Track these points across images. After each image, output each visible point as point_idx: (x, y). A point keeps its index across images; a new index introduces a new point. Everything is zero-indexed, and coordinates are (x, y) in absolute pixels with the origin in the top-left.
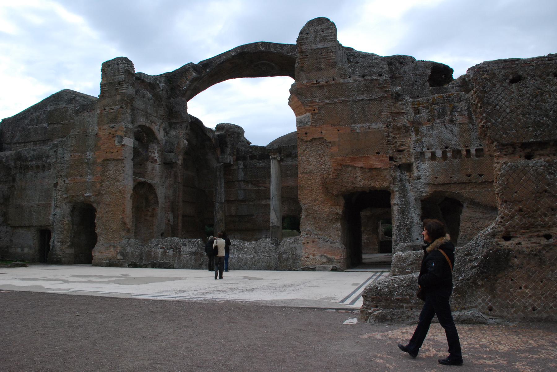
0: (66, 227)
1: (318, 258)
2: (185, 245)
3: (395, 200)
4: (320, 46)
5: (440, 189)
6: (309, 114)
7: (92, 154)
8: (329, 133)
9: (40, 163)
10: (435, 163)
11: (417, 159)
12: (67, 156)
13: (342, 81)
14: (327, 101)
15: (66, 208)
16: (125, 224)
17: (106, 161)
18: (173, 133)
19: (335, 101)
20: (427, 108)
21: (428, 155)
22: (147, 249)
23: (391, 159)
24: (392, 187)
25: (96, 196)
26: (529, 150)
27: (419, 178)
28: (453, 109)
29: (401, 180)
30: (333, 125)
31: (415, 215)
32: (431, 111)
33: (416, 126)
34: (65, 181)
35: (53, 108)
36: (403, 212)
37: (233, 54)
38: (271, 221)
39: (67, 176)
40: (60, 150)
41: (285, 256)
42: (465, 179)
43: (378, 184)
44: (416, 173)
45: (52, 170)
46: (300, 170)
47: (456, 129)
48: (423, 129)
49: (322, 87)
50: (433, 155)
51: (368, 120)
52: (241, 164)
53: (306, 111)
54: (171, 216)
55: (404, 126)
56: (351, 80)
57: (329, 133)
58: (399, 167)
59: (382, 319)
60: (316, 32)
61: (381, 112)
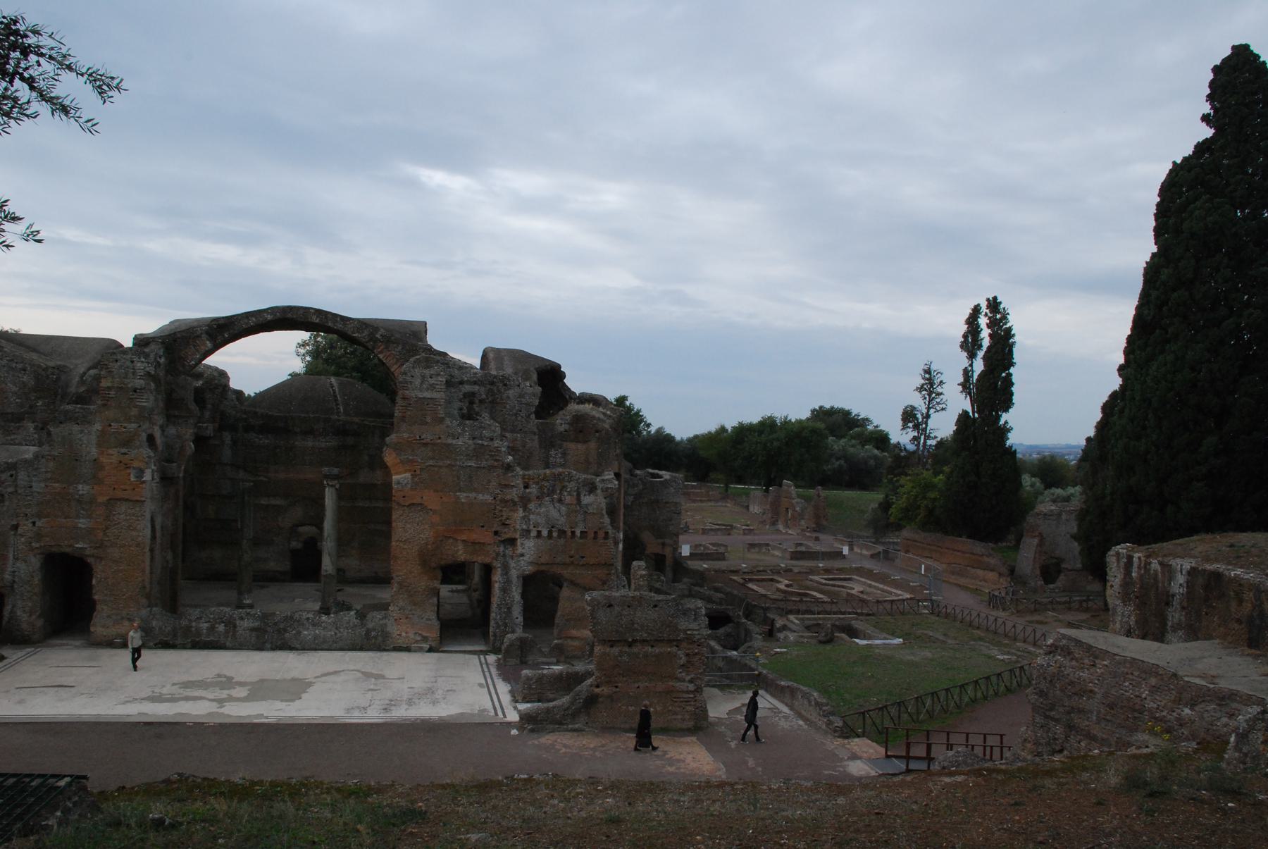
0: (36, 590)
1: (411, 636)
2: (242, 619)
4: (427, 395)
5: (543, 568)
6: (408, 475)
7: (87, 488)
8: (431, 499)
10: (540, 541)
11: (522, 536)
12: (38, 487)
13: (450, 441)
14: (431, 462)
15: (35, 562)
16: (144, 587)
17: (113, 501)
18: (172, 430)
19: (440, 463)
20: (537, 483)
21: (534, 534)
22: (184, 623)
23: (496, 533)
24: (495, 564)
25: (96, 548)
26: (612, 643)
27: (522, 555)
28: (564, 487)
29: (504, 556)
30: (436, 491)
31: (516, 594)
32: (541, 488)
33: (525, 501)
34: (34, 523)
36: (505, 590)
37: (269, 317)
38: (324, 567)
39: (39, 516)
40: (22, 475)
41: (373, 634)
42: (568, 560)
44: (520, 550)
45: (7, 503)
46: (394, 538)
47: (563, 509)
48: (531, 506)
49: (426, 445)
50: (539, 532)
51: (475, 490)
52: (227, 437)
53: (406, 472)
54: (169, 556)
55: (512, 500)
58: (503, 542)
59: (532, 731)
60: (423, 377)
61: (489, 481)
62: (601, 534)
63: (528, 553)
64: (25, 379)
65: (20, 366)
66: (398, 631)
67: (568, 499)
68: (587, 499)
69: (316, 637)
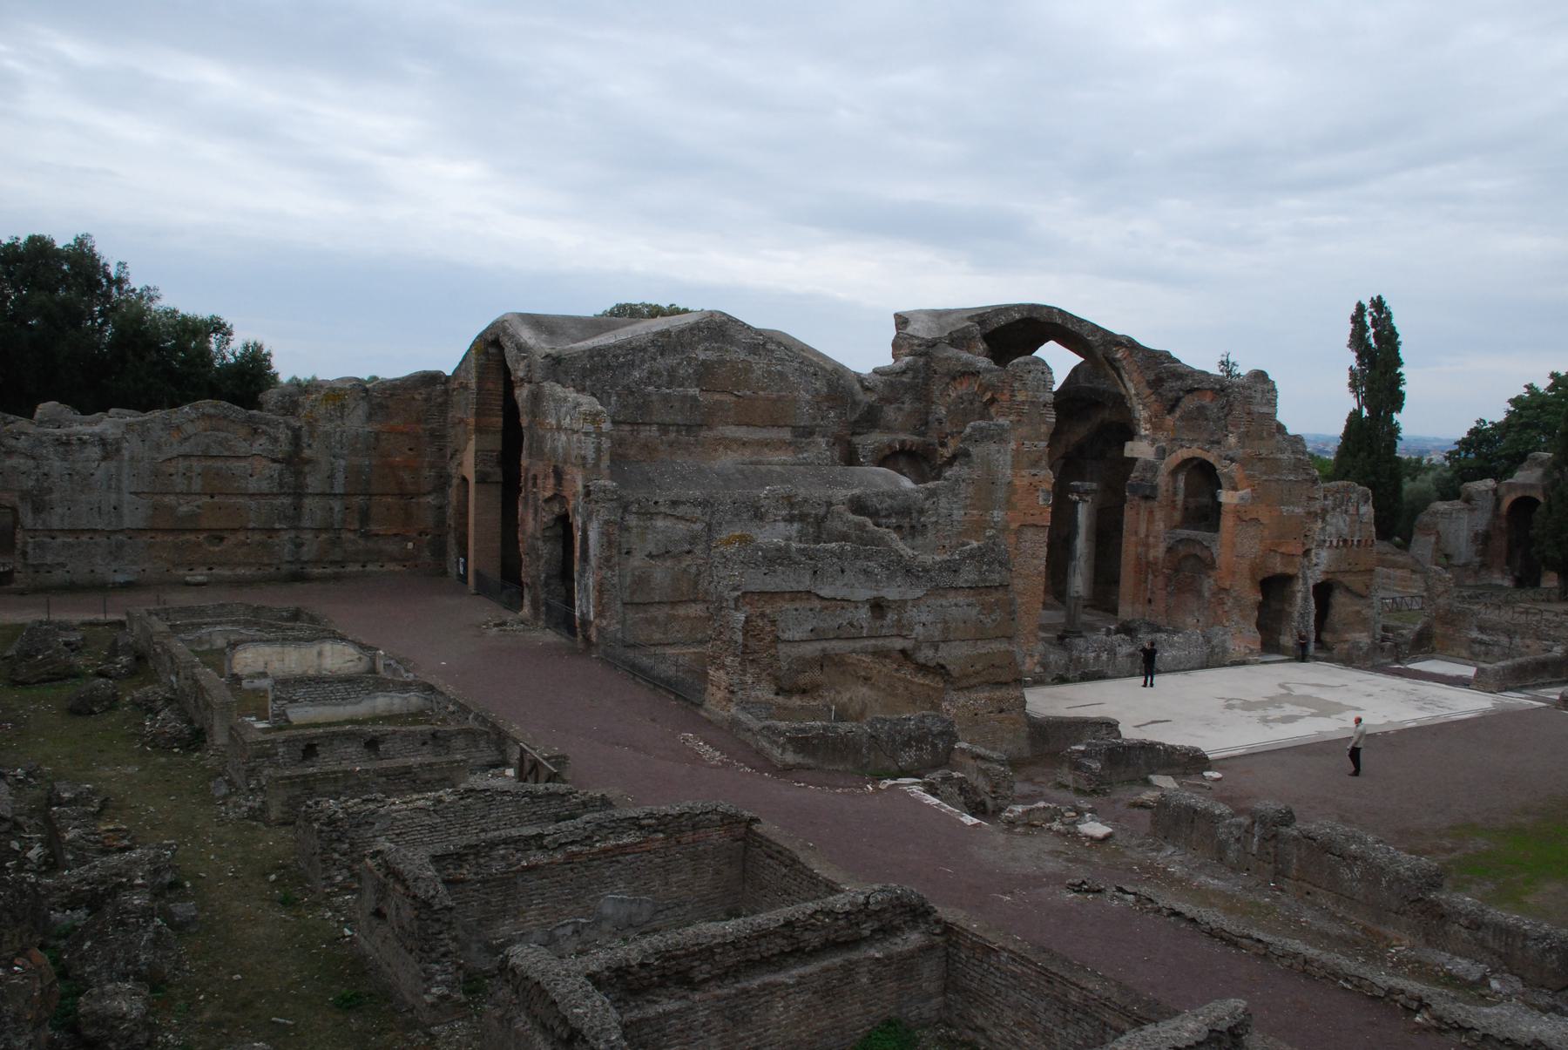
3: (1299, 586)
4: (1265, 410)
9: (906, 522)
12: (958, 514)
33: (1325, 511)
35: (712, 356)
36: (1305, 599)
37: (1017, 316)
40: (943, 502)
43: (1290, 571)
48: (1328, 517)
56: (1284, 457)
57: (1264, 515)
63: (1323, 561)
64: (818, 385)
65: (812, 370)
66: (1236, 647)
67: (1352, 510)
69: (1174, 658)
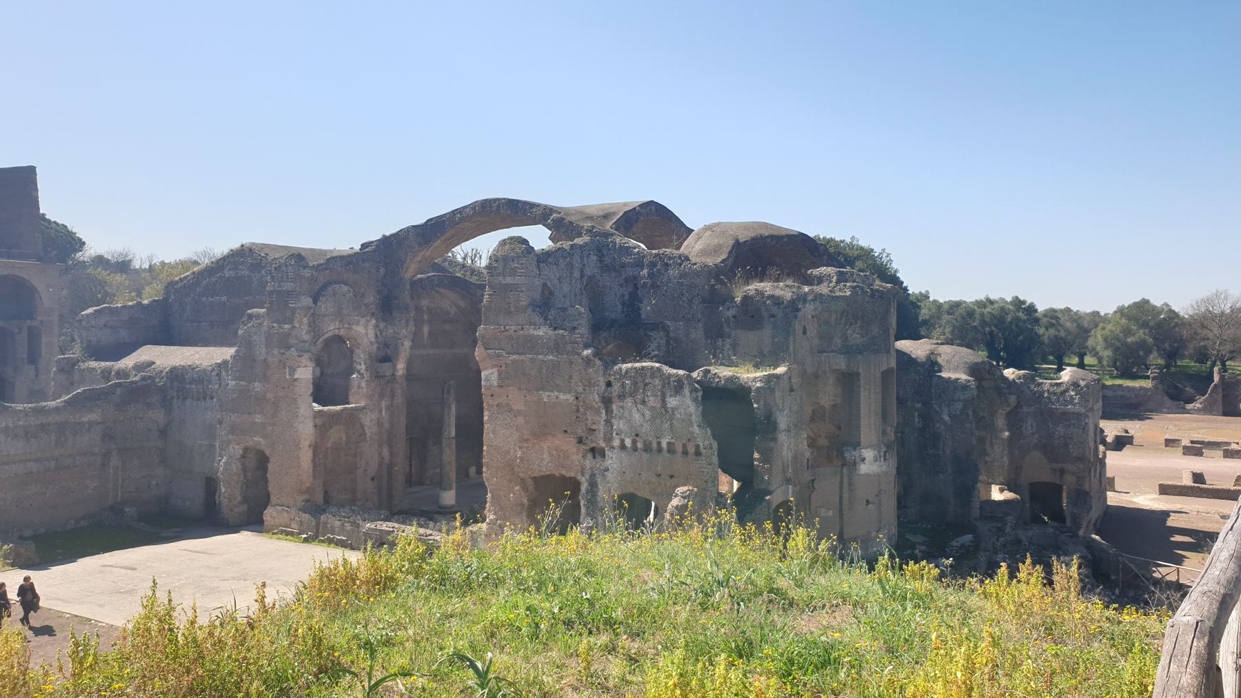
4: (509, 280)
6: (495, 370)
62: (691, 450)
68: (672, 402)
